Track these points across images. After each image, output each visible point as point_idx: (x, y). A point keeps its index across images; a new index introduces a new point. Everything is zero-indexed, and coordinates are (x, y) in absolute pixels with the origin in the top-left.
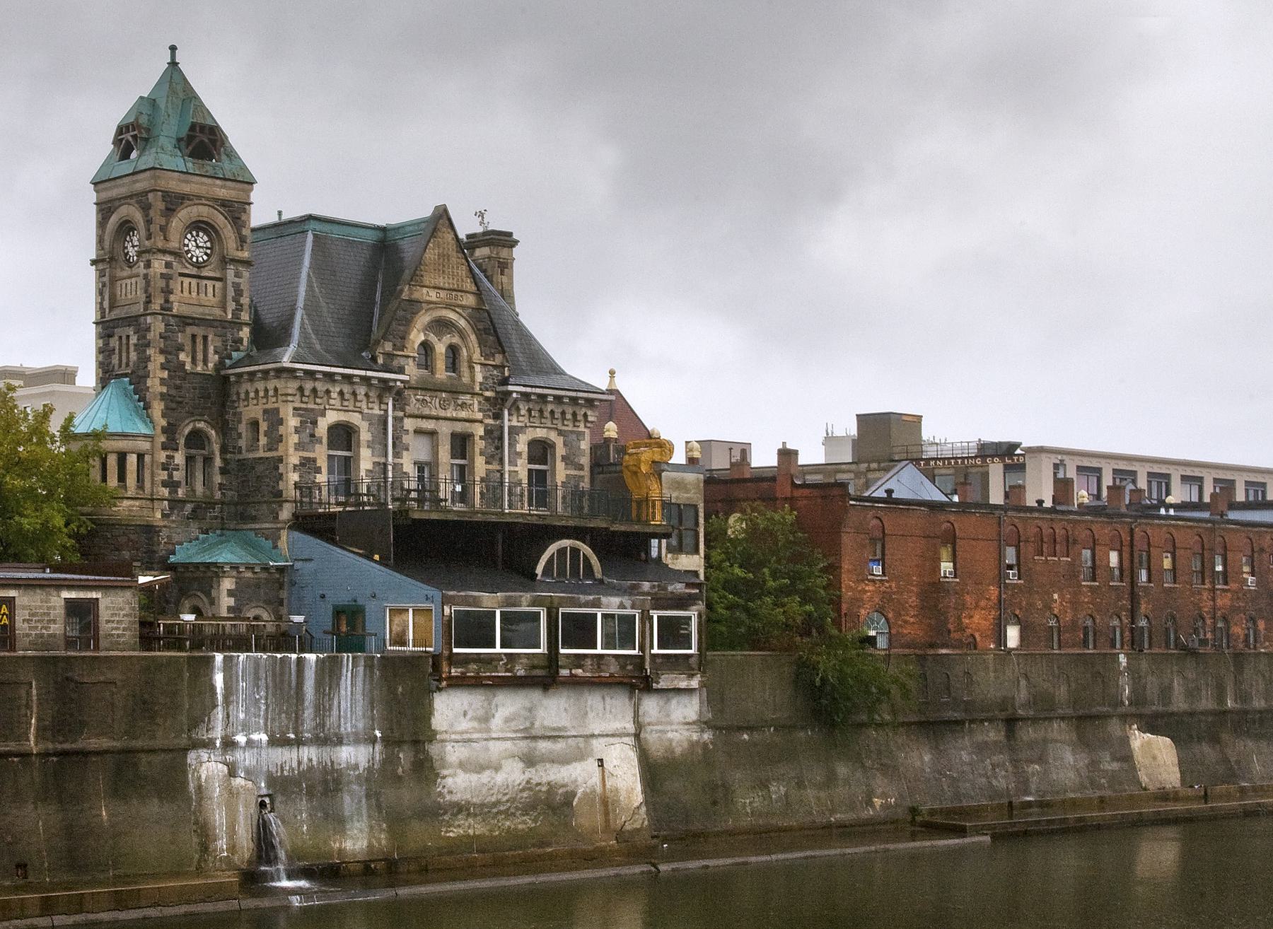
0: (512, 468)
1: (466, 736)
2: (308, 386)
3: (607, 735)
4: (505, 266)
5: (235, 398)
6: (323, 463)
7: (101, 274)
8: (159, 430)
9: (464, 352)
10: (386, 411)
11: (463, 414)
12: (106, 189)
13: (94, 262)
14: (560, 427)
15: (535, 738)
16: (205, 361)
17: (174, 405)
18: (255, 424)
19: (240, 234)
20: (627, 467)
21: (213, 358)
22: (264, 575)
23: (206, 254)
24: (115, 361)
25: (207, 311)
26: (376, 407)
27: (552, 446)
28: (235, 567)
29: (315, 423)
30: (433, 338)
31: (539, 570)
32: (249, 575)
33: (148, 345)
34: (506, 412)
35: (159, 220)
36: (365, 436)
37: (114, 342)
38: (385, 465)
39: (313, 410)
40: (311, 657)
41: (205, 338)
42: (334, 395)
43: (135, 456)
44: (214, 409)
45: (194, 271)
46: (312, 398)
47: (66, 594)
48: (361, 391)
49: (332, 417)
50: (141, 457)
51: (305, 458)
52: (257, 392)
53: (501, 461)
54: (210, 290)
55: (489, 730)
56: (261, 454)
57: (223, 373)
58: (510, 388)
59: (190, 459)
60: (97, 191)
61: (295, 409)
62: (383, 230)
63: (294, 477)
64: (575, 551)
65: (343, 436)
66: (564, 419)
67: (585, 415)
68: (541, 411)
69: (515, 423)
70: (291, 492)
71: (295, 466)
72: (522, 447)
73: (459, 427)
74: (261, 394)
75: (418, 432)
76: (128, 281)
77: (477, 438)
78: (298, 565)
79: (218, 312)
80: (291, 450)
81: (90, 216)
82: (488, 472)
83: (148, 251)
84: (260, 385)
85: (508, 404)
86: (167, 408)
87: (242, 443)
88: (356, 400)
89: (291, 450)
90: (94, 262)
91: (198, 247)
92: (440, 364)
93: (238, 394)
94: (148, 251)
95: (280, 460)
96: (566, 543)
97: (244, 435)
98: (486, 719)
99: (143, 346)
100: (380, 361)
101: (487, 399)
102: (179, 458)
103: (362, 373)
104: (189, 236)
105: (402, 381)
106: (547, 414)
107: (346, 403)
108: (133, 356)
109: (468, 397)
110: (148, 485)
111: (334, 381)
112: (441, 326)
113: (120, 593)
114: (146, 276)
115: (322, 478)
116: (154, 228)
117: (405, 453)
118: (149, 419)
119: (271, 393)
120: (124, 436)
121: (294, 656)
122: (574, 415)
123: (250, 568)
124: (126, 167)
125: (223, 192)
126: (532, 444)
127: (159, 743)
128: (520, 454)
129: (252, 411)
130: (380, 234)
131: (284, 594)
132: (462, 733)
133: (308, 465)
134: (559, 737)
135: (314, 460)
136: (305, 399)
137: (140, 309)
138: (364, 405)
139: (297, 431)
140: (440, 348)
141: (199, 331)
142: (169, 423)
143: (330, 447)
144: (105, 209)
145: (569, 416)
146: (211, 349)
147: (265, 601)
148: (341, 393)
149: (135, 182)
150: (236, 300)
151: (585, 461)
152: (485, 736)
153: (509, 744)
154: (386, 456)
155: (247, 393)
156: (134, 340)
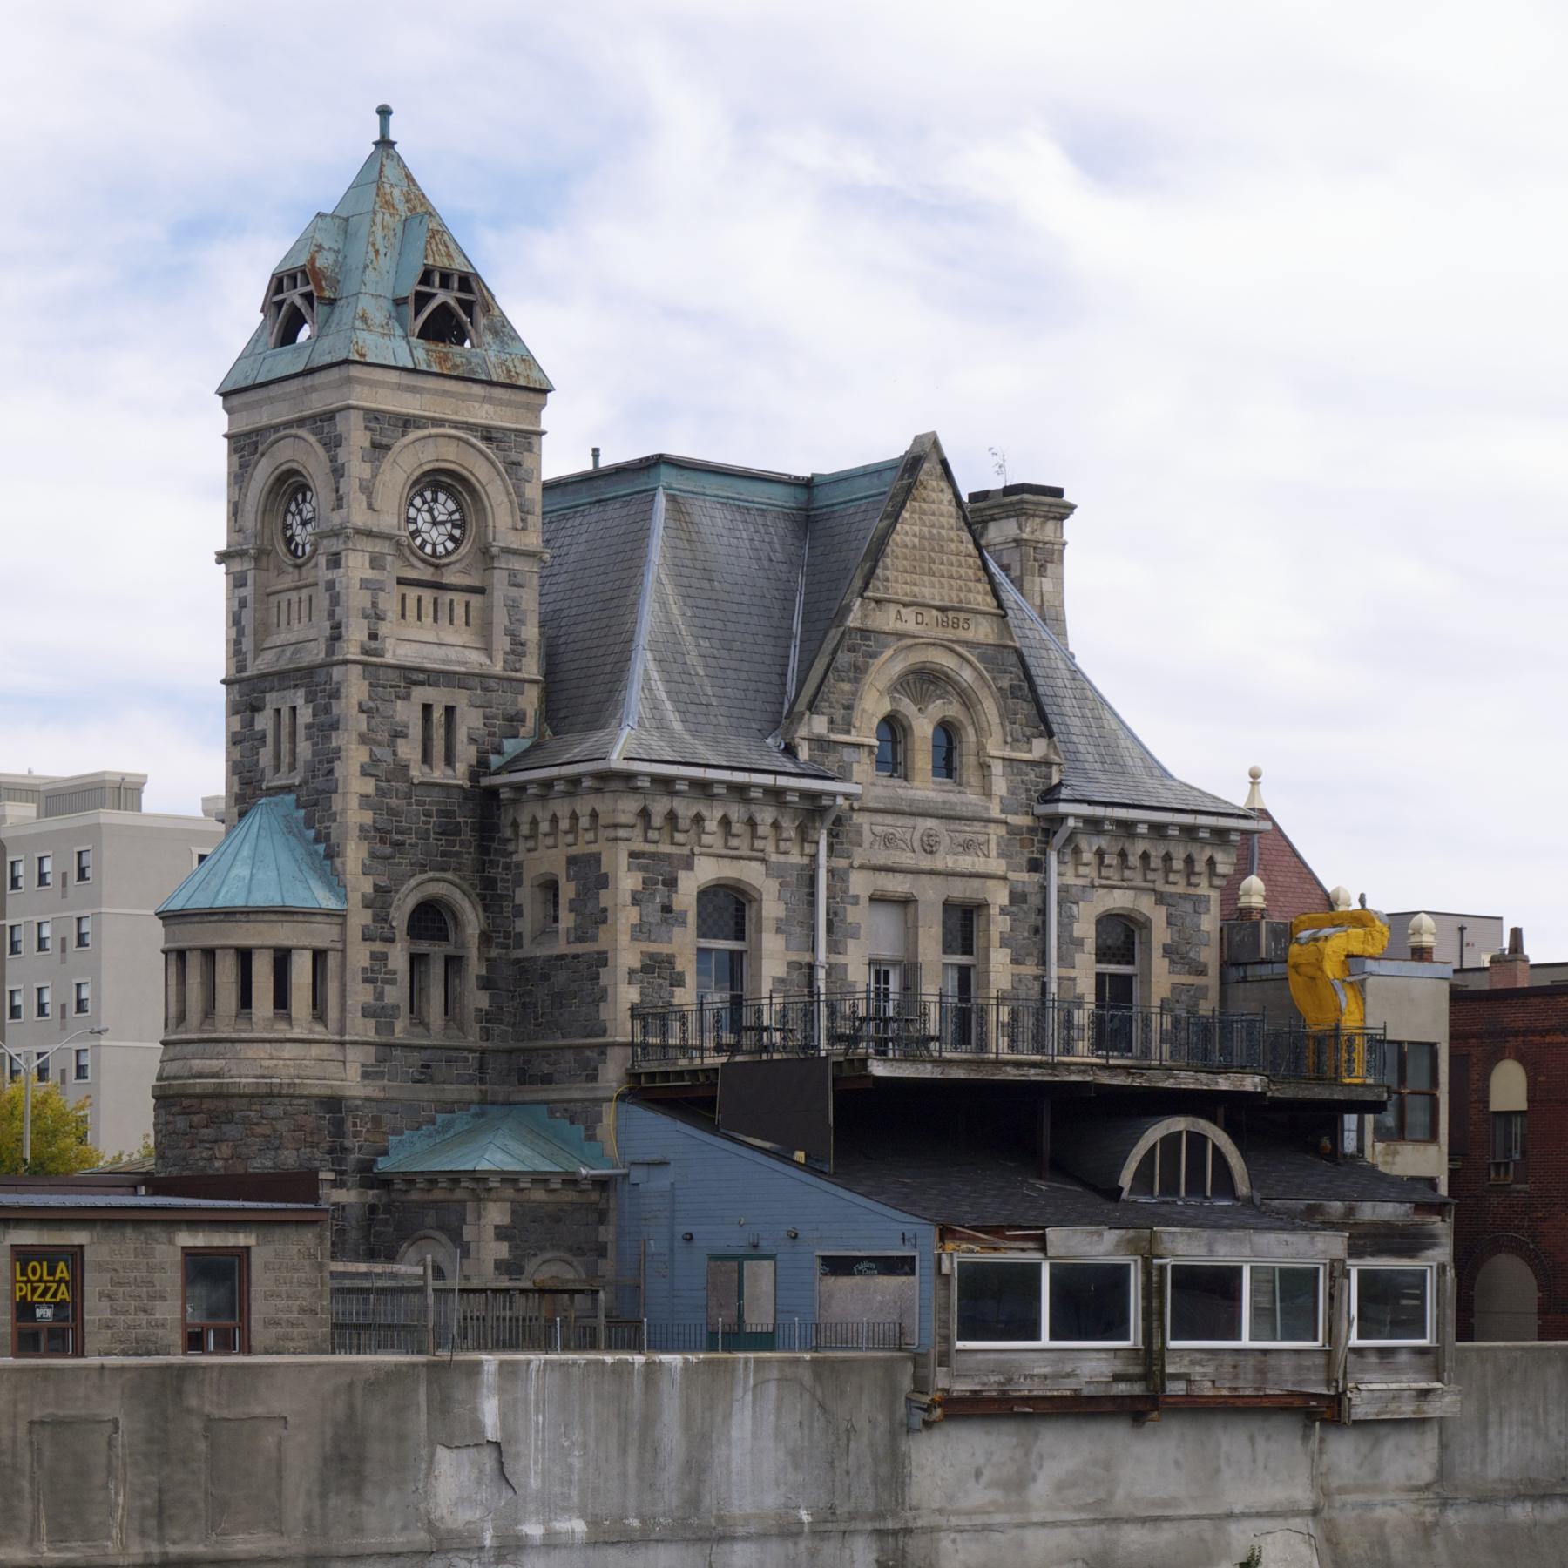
0: (1065, 972)
1: (979, 1520)
2: (660, 806)
3: (1259, 1515)
4: (1049, 557)
5: (508, 833)
6: (687, 965)
7: (237, 581)
8: (355, 899)
9: (970, 736)
10: (814, 857)
11: (966, 863)
12: (248, 407)
13: (222, 557)
14: (1160, 886)
15: (1116, 1521)
16: (449, 760)
17: (388, 850)
18: (551, 887)
19: (520, 495)
20: (1296, 967)
21: (466, 754)
22: (571, 1195)
23: (451, 537)
24: (265, 757)
25: (452, 654)
26: (795, 850)
27: (1145, 925)
28: (510, 1179)
29: (671, 883)
30: (907, 707)
31: (1126, 1179)
32: (539, 1195)
33: (334, 726)
34: (1053, 858)
35: (358, 469)
36: (772, 907)
37: (264, 721)
38: (812, 967)
39: (670, 855)
40: (673, 1359)
41: (450, 711)
42: (711, 826)
43: (308, 955)
44: (468, 859)
45: (425, 574)
46: (667, 829)
47: (185, 1239)
48: (766, 816)
49: (707, 871)
50: (319, 956)
51: (651, 956)
52: (554, 820)
53: (1043, 961)
54: (460, 611)
55: (1024, 1507)
56: (562, 947)
57: (485, 781)
58: (1063, 808)
59: (416, 960)
60: (229, 410)
61: (632, 855)
62: (808, 485)
63: (629, 995)
64: (1197, 1141)
65: (729, 908)
66: (1168, 870)
67: (1211, 862)
68: (1123, 855)
69: (1070, 880)
70: (622, 1028)
71: (632, 972)
72: (1085, 930)
73: (960, 890)
74: (564, 824)
75: (877, 899)
76: (294, 596)
77: (995, 911)
78: (637, 1175)
79: (475, 659)
80: (624, 939)
81: (217, 459)
82: (1017, 980)
83: (335, 533)
84: (562, 808)
85: (1059, 840)
86: (373, 855)
87: (524, 927)
88: (754, 836)
89: (624, 939)
90: (222, 557)
91: (435, 523)
92: (923, 759)
93: (515, 825)
94: (335, 533)
95: (602, 959)
96: (1179, 1124)
97: (527, 910)
98: (1018, 1484)
99: (326, 726)
100: (804, 753)
101: (1014, 831)
102: (398, 958)
103: (768, 780)
104: (418, 501)
105: (847, 796)
106: (1133, 860)
107: (734, 842)
108: (304, 748)
109: (978, 826)
110: (333, 1013)
111: (712, 797)
112: (924, 681)
113: (291, 1232)
114: (331, 585)
115: (685, 996)
116: (350, 486)
117: (851, 943)
118: (334, 880)
119: (584, 822)
120: (286, 913)
121: (639, 1359)
122: (1189, 861)
123: (540, 1179)
124: (287, 361)
125: (485, 415)
126: (1106, 921)
127: (372, 1542)
128: (1079, 943)
129: (543, 859)
130: (802, 495)
131: (607, 1234)
132: (969, 1513)
133: (657, 968)
134: (1166, 1519)
135: (669, 960)
136: (652, 835)
137: (316, 653)
138: (770, 847)
139: (636, 900)
140: (923, 728)
141: (438, 697)
142: (377, 888)
143: (702, 934)
144: (245, 447)
145: (1178, 864)
146: (461, 734)
147: (570, 1249)
148: (725, 822)
149: (308, 391)
150: (513, 635)
151: (1210, 955)
152: (1018, 1518)
153: (1062, 1536)
154: (813, 949)
155: (534, 822)
156: (305, 715)
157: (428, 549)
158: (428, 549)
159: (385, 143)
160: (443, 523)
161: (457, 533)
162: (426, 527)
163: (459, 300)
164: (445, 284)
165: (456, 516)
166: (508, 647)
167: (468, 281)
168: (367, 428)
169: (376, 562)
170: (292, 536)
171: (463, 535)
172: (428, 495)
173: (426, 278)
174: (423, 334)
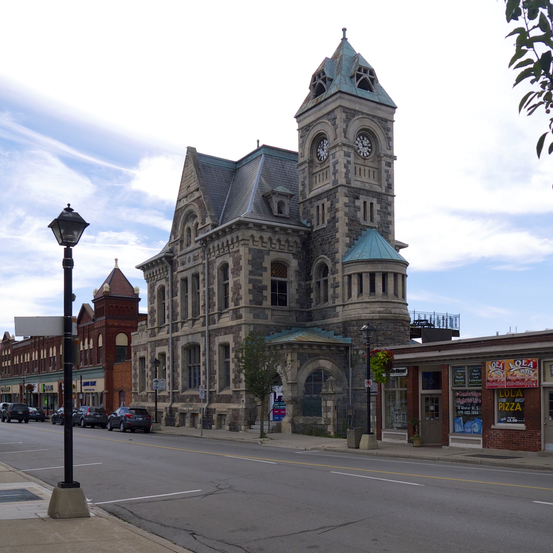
23: (368, 151)
104: (358, 139)
157: (362, 154)
158: (362, 154)
159: (344, 39)
160: (366, 146)
161: (370, 150)
162: (361, 147)
163: (370, 78)
164: (365, 72)
165: (369, 145)
166: (386, 185)
167: (372, 72)
168: (344, 112)
169: (347, 155)
170: (320, 155)
171: (372, 150)
172: (361, 137)
173: (359, 70)
174: (359, 87)
